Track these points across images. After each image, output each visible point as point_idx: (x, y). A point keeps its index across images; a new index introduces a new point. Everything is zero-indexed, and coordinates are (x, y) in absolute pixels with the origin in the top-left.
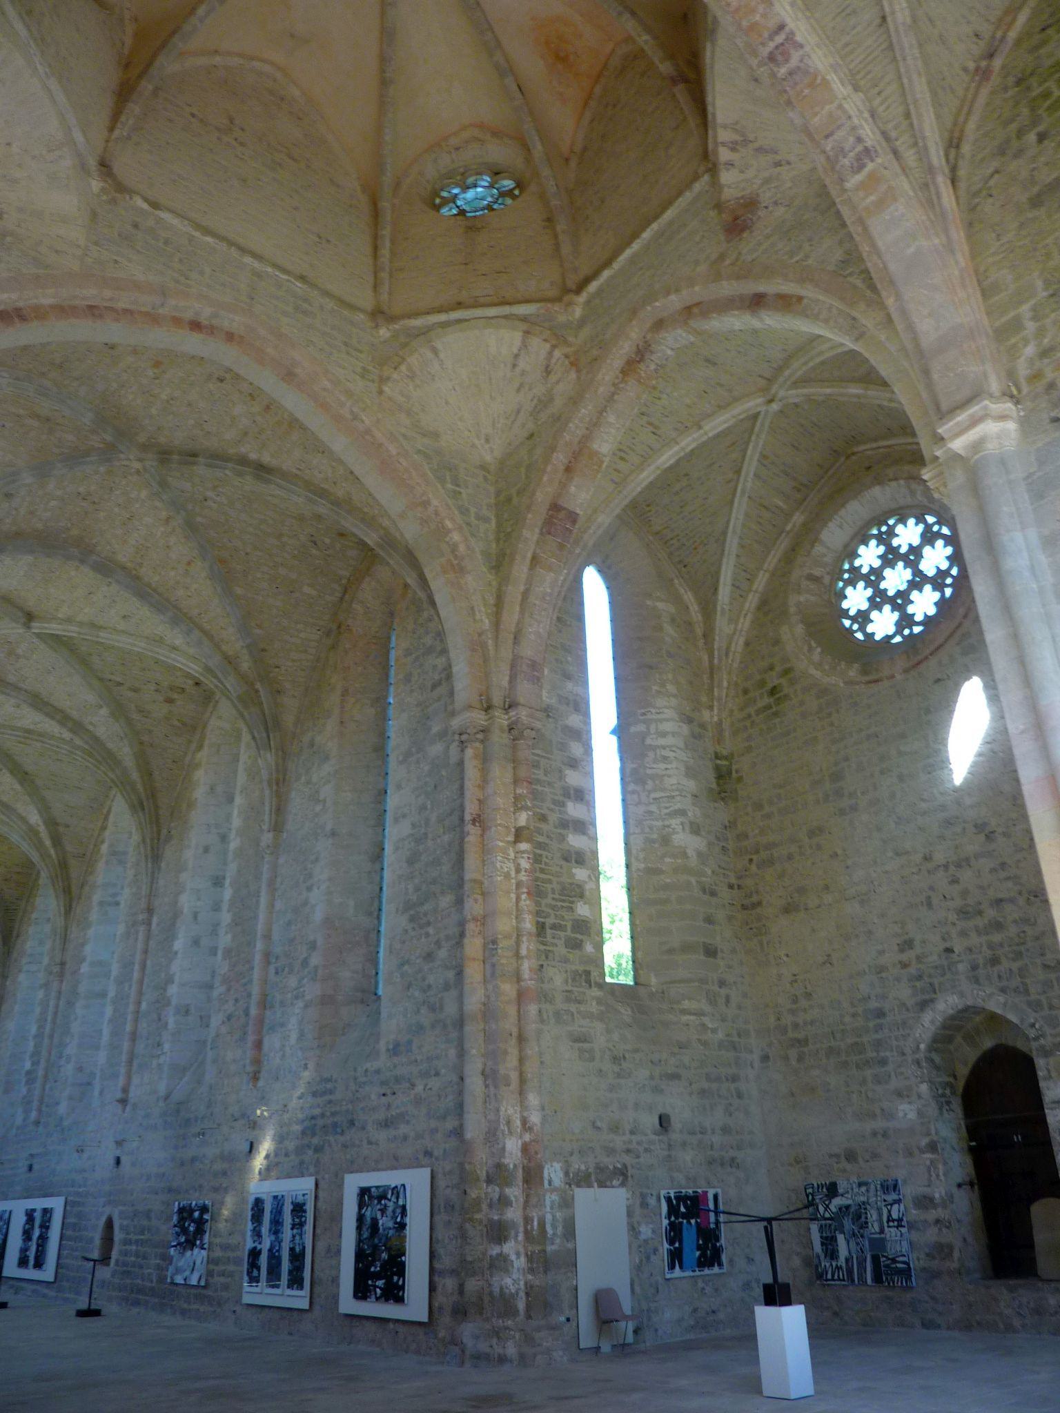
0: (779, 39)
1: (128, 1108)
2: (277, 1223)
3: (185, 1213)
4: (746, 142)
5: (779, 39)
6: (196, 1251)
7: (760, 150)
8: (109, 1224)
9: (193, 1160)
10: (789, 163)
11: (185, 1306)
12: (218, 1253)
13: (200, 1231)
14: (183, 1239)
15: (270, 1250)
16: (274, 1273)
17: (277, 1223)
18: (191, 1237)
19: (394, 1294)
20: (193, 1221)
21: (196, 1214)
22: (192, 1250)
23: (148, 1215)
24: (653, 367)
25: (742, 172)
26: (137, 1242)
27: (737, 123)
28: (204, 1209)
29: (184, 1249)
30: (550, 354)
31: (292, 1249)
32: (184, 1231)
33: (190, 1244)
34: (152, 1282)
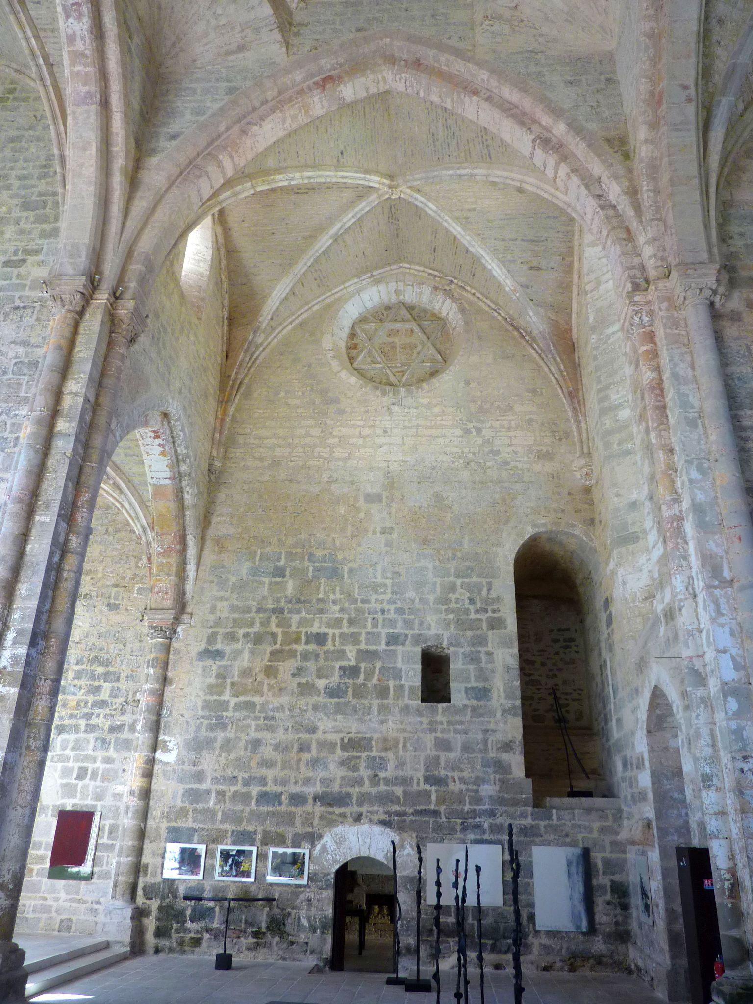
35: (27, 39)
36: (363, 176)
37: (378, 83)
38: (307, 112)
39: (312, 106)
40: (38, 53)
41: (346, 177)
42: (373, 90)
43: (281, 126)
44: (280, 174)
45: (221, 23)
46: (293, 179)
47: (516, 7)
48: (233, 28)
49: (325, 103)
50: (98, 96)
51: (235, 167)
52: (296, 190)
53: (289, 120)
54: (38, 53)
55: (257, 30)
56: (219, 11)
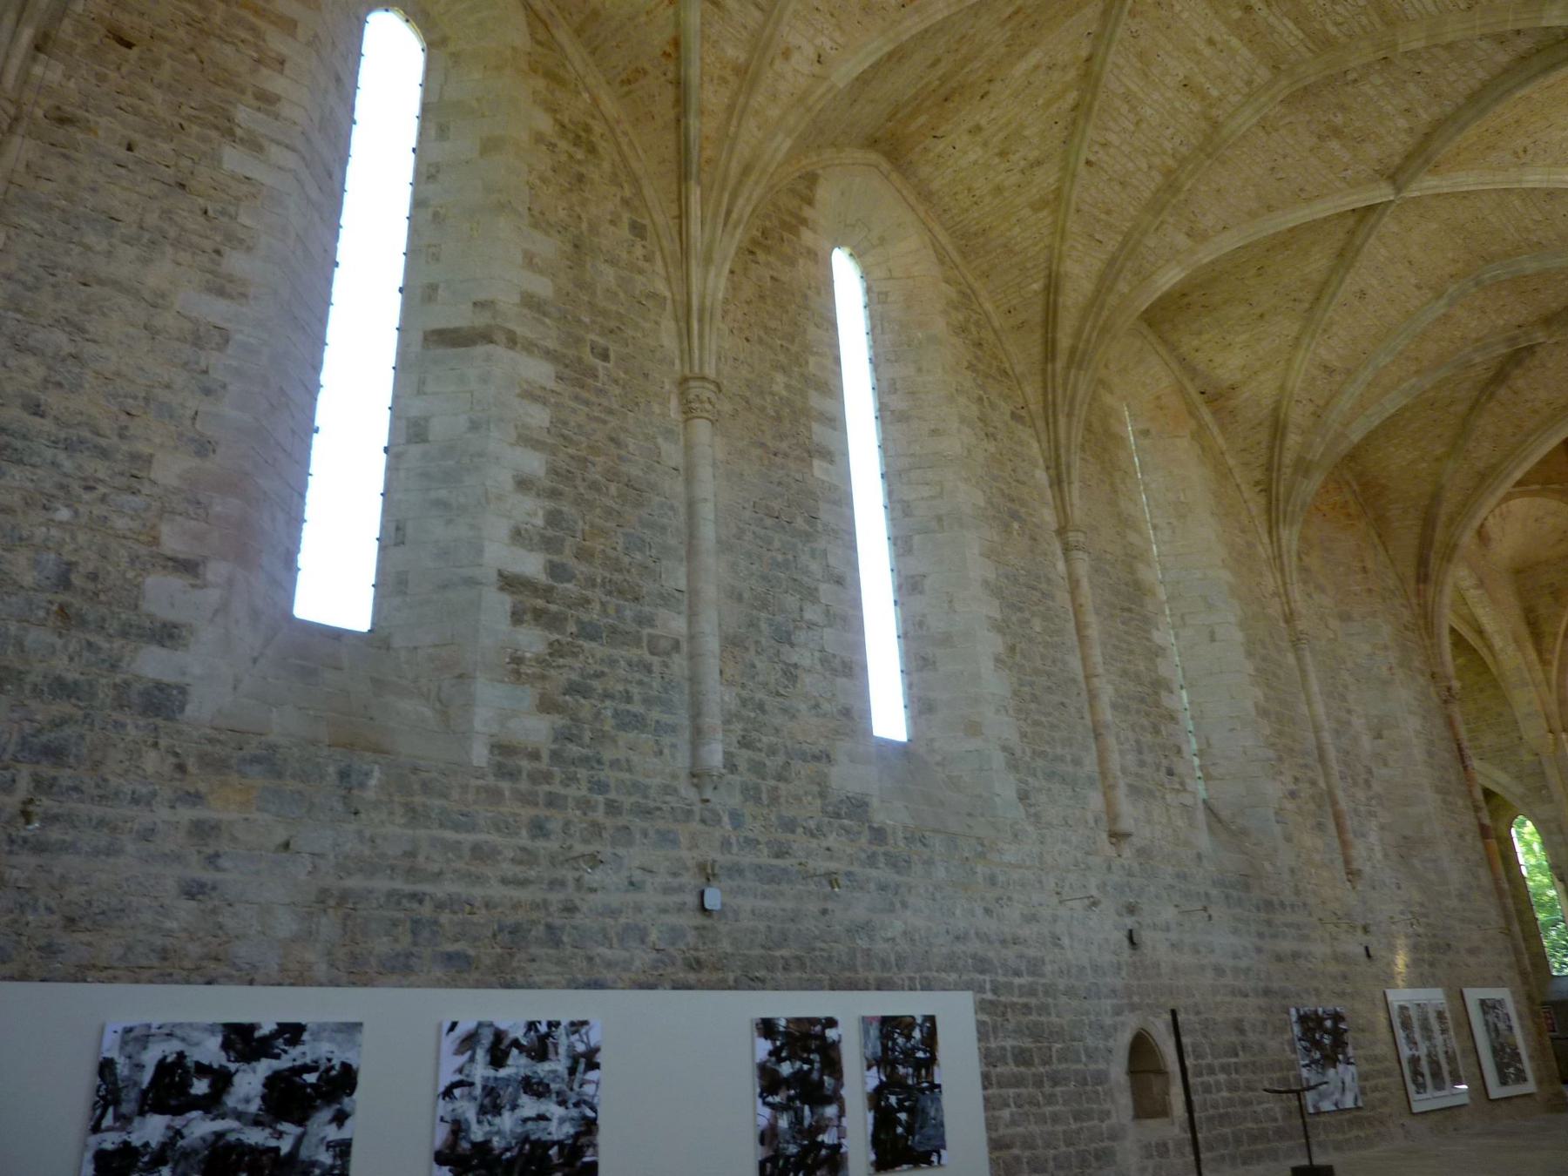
1: (1127, 852)
2: (1426, 1028)
3: (1310, 1023)
6: (1341, 1067)
8: (1141, 1047)
9: (1296, 955)
11: (1340, 1137)
12: (1366, 1067)
13: (1339, 1041)
14: (1317, 1055)
15: (1429, 1055)
16: (1436, 1074)
17: (1426, 1028)
18: (1329, 1052)
19: (1521, 1077)
20: (1326, 1031)
21: (1328, 1023)
22: (1335, 1067)
23: (1239, 1028)
26: (1225, 1069)
28: (1337, 1017)
29: (1323, 1067)
31: (1446, 1052)
32: (1317, 1044)
33: (1330, 1059)
34: (1275, 1120)
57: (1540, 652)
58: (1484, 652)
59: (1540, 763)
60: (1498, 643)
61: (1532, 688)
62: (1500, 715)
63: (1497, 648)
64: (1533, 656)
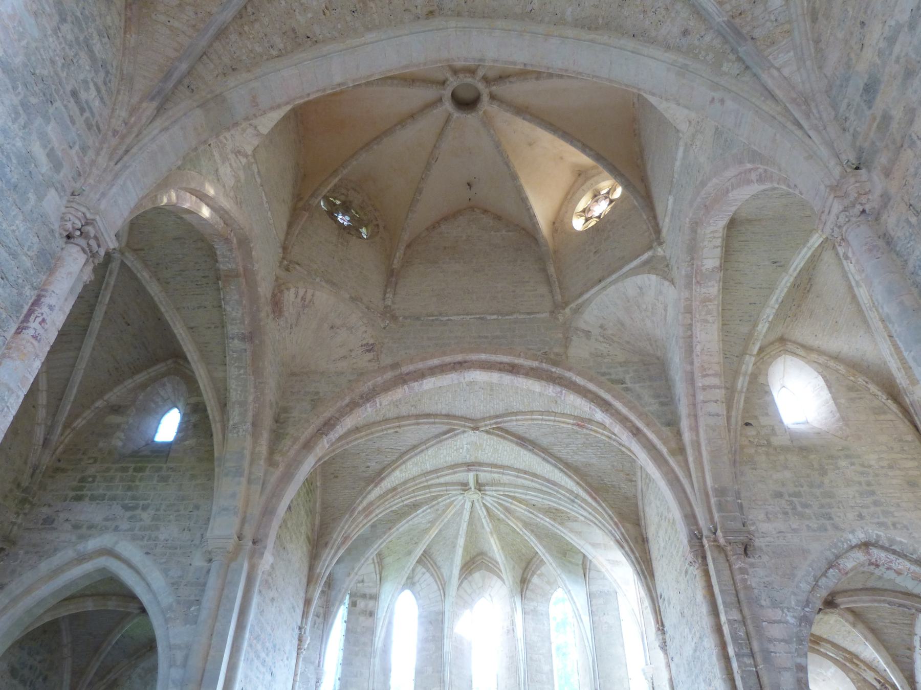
0: (378, 405)
4: (304, 307)
5: (378, 405)
7: (299, 315)
10: (290, 334)
24: (216, 240)
25: (293, 302)
27: (313, 303)
30: (246, 156)
35: (602, 434)
36: (805, 249)
37: (714, 238)
38: (710, 301)
39: (707, 295)
40: (610, 435)
41: (797, 266)
42: (718, 242)
43: (709, 325)
44: (757, 326)
45: (651, 310)
46: (768, 317)
47: (690, 122)
48: (655, 305)
49: (710, 284)
50: (630, 434)
51: (716, 375)
52: (806, 291)
53: (709, 318)
54: (610, 435)
55: (661, 292)
56: (644, 307)
57: (272, 452)
58: (216, 428)
59: (208, 571)
60: (235, 416)
61: (244, 480)
62: (197, 507)
63: (231, 423)
64: (264, 449)
